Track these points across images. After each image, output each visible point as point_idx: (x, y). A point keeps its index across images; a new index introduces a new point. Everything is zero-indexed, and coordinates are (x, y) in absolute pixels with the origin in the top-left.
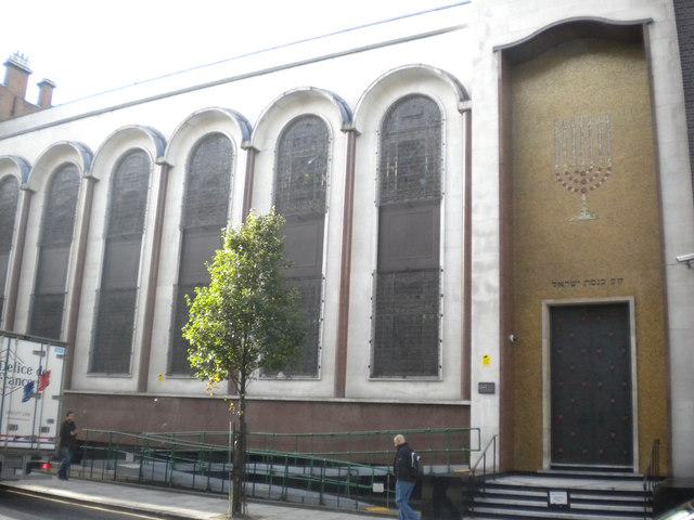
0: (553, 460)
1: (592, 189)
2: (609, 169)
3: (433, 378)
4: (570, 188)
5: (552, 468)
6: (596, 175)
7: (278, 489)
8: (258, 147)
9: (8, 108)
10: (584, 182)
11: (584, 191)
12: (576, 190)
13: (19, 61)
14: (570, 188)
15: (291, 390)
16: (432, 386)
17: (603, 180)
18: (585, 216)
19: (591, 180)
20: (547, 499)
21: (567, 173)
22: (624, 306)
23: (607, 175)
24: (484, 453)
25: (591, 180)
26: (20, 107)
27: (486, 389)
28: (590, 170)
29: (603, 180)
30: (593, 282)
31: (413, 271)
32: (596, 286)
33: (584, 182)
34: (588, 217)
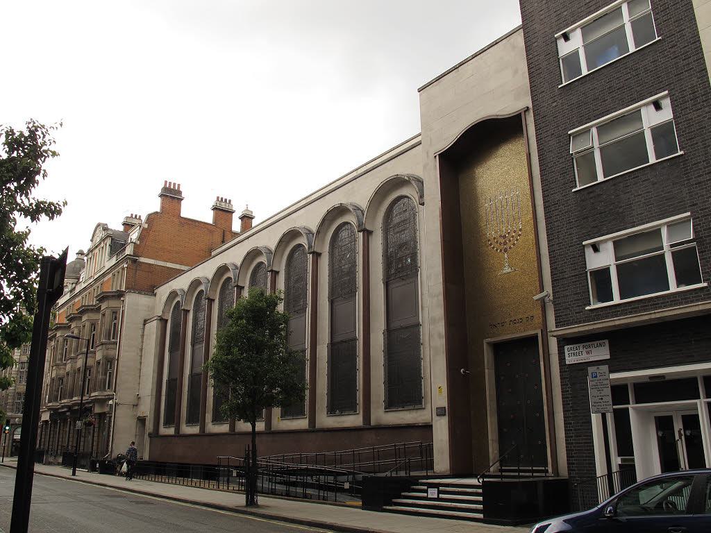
0: (501, 466)
1: (510, 248)
2: (520, 230)
3: (419, 406)
4: (497, 250)
5: (501, 471)
6: (513, 237)
7: (300, 490)
8: (319, 251)
9: (220, 239)
10: (505, 243)
11: (506, 250)
12: (501, 251)
13: (223, 205)
14: (497, 250)
15: (343, 422)
16: (420, 412)
17: (517, 240)
18: (507, 270)
19: (510, 241)
20: (439, 492)
21: (494, 238)
22: (535, 338)
23: (519, 235)
24: (442, 461)
25: (510, 241)
26: (228, 235)
27: (441, 412)
28: (509, 233)
29: (517, 240)
30: (514, 322)
31: (407, 328)
32: (517, 325)
33: (505, 243)
34: (510, 270)
